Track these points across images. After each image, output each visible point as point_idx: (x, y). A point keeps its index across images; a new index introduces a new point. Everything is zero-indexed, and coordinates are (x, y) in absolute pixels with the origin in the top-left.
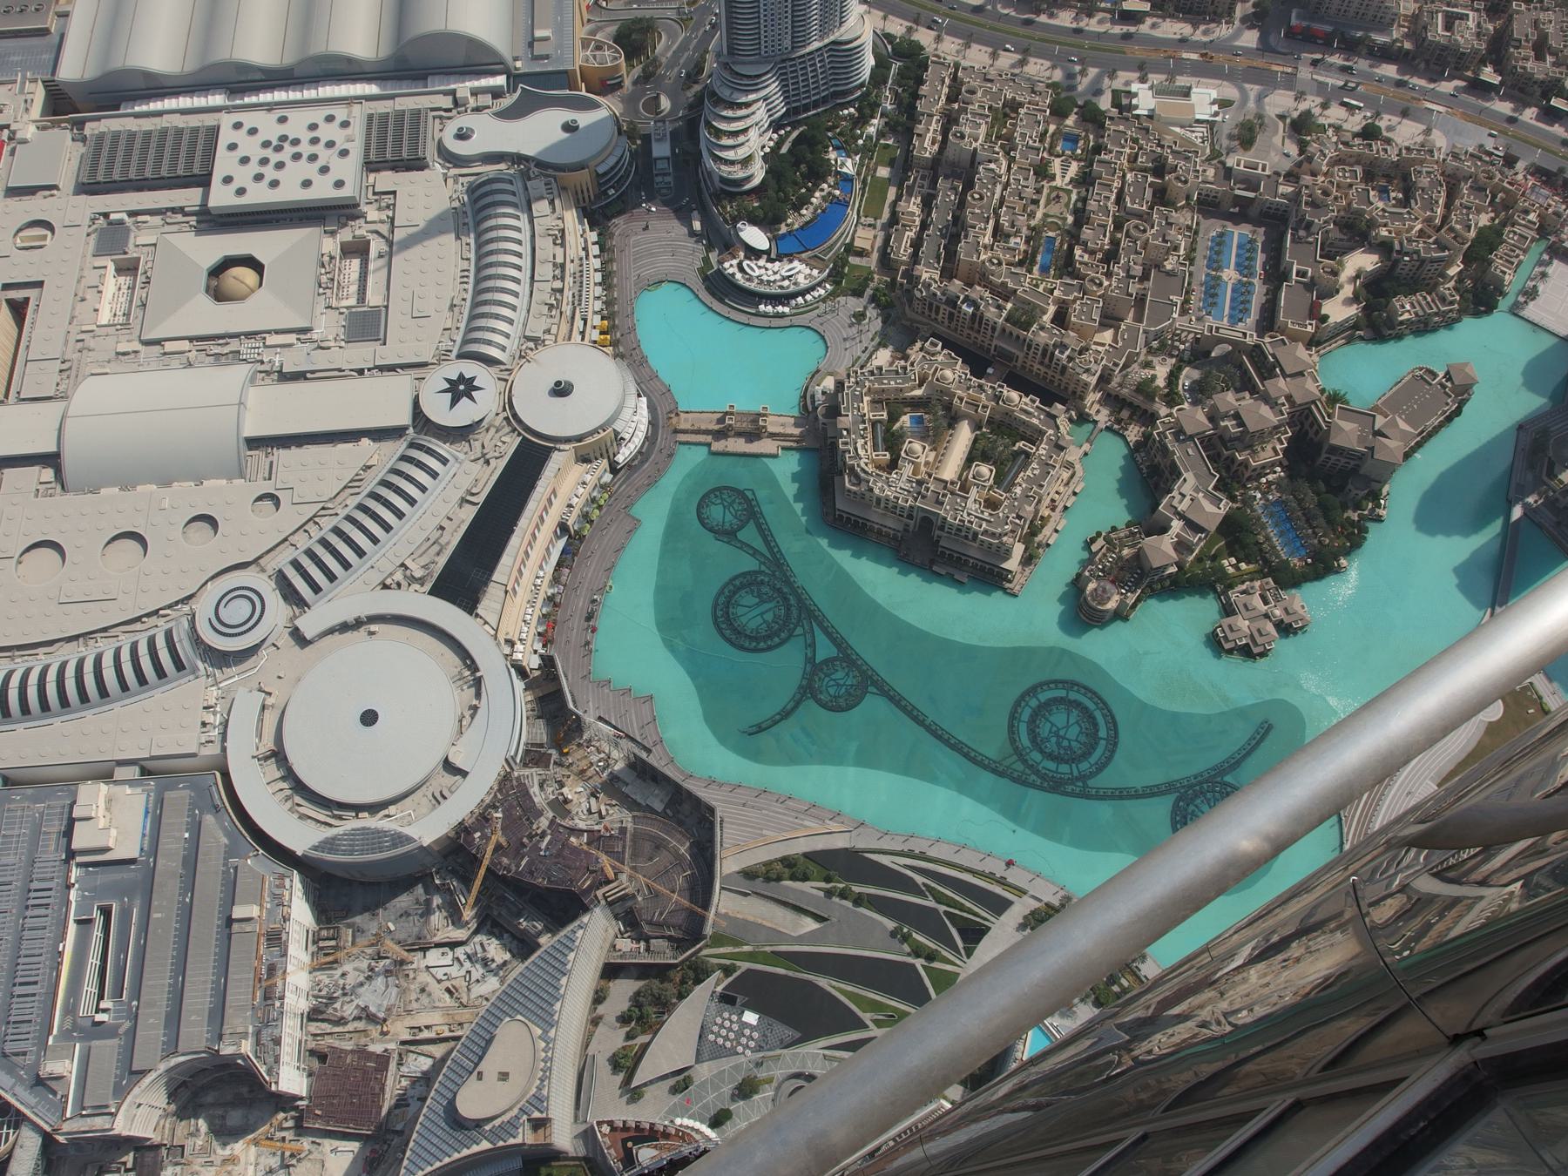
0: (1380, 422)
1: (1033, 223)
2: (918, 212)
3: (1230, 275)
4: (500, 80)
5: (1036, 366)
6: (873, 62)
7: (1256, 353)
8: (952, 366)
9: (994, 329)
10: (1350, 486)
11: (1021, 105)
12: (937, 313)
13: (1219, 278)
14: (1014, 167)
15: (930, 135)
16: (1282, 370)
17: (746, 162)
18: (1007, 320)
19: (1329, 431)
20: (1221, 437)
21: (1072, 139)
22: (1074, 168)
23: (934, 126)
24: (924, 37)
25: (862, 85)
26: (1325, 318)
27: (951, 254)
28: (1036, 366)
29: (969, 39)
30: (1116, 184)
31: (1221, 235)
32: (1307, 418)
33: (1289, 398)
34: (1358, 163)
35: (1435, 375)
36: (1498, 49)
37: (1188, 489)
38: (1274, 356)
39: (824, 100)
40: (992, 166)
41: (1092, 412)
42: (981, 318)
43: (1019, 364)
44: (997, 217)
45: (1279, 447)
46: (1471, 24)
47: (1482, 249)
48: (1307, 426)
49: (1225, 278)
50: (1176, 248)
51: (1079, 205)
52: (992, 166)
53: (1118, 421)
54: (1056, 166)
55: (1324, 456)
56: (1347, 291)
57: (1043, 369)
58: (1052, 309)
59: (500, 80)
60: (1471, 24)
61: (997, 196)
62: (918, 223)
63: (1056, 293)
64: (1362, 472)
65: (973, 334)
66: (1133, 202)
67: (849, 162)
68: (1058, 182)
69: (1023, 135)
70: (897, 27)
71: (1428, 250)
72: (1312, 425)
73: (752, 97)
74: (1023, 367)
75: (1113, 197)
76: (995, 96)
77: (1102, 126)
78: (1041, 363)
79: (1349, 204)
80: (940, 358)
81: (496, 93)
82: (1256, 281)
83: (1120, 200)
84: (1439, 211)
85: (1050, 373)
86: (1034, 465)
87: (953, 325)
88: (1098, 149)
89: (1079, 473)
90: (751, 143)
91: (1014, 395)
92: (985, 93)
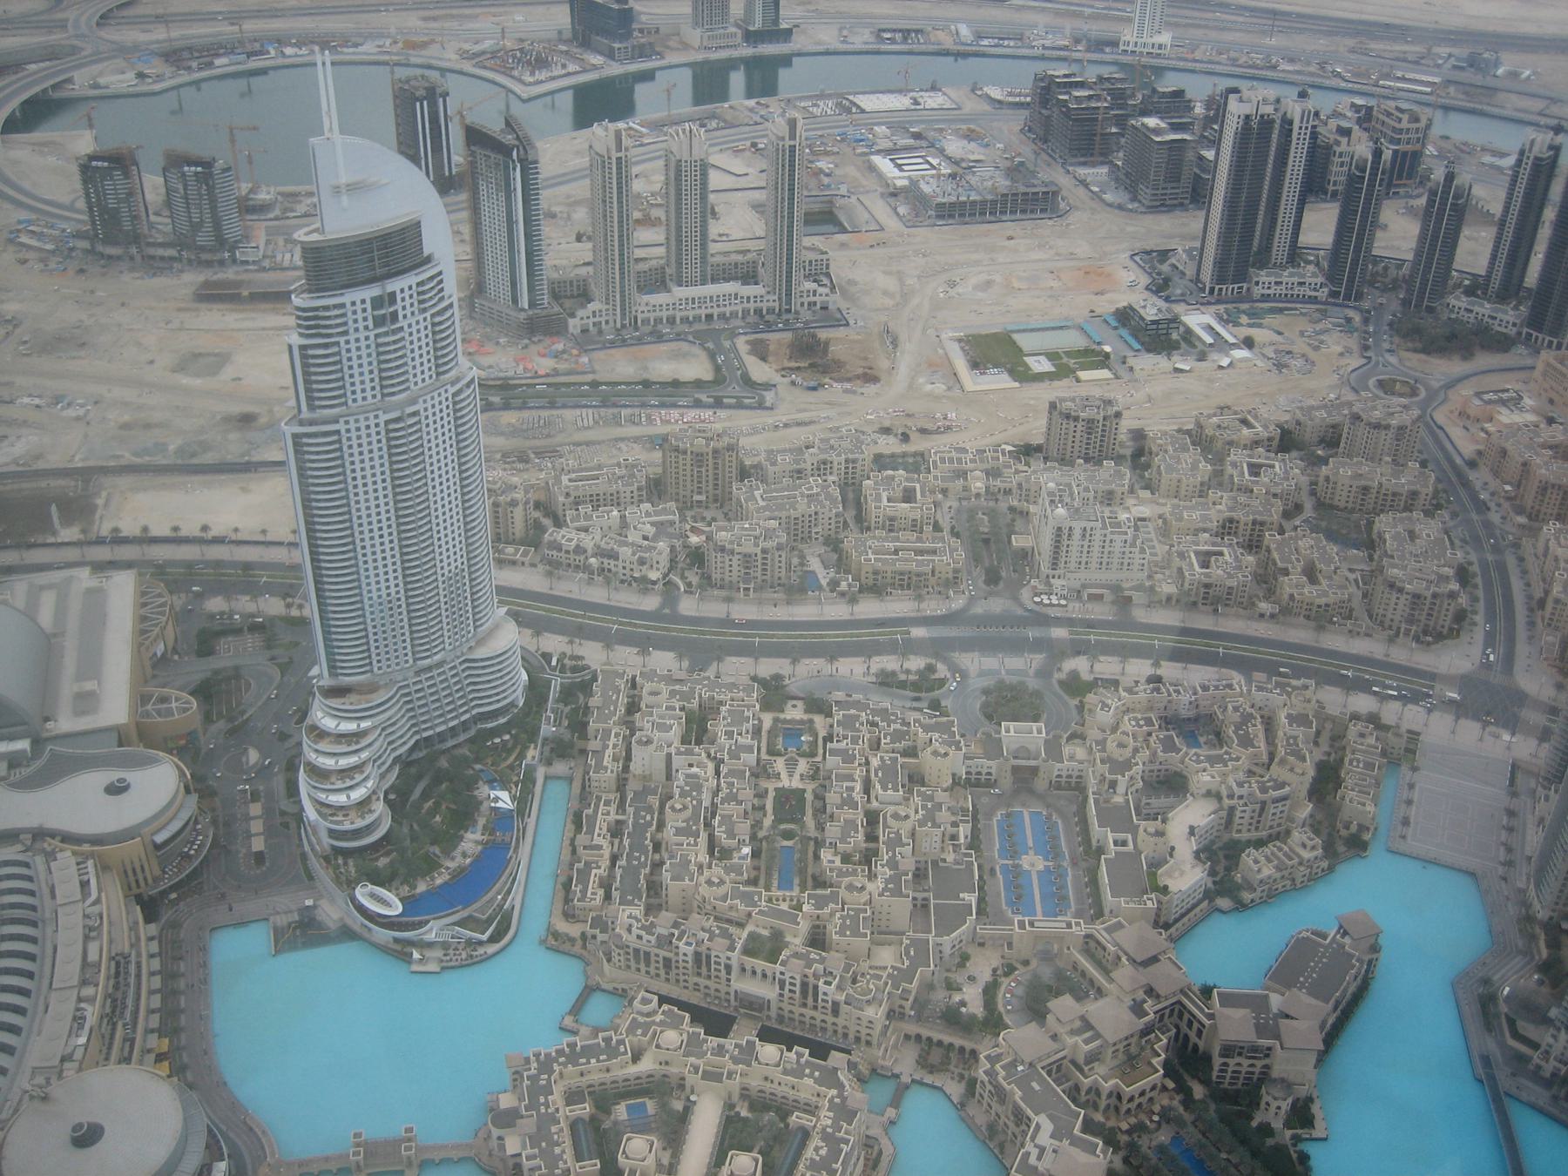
0: (1276, 1001)
1: (761, 834)
2: (605, 844)
3: (1033, 863)
4: (23, 745)
5: (798, 1010)
6: (525, 677)
7: (1091, 946)
8: (676, 1025)
9: (728, 968)
10: (1266, 1098)
11: (721, 703)
12: (648, 965)
13: (1017, 866)
14: (724, 770)
15: (609, 752)
16: (1130, 959)
17: (363, 805)
18: (747, 951)
19: (1214, 1027)
20: (1073, 1062)
21: (792, 731)
22: (803, 766)
23: (613, 740)
24: (593, 654)
25: (513, 704)
26: (1165, 890)
27: (654, 888)
28: (798, 1010)
29: (644, 644)
30: (859, 773)
31: (1008, 815)
32: (1181, 1016)
33: (1150, 991)
34: (1151, 709)
35: (1324, 937)
36: (1267, 578)
37: (1044, 1138)
38: (1117, 945)
39: (465, 726)
40: (695, 770)
41: (888, 1063)
42: (708, 957)
43: (773, 1013)
44: (708, 825)
45: (1155, 1061)
46: (1227, 557)
47: (1327, 780)
48: (1184, 1029)
49: (1026, 867)
50: (954, 837)
51: (819, 804)
52: (695, 770)
53: (932, 1069)
54: (780, 765)
55: (1217, 1061)
56: (1186, 849)
57: (809, 1012)
58: (804, 926)
59: (23, 745)
60: (1227, 557)
61: (706, 803)
62: (606, 853)
63: (805, 908)
64: (1275, 1074)
65: (702, 981)
66: (885, 789)
67: (504, 795)
68: (785, 782)
69: (729, 734)
70: (554, 644)
71: (1264, 790)
72: (1190, 1024)
73: (365, 724)
74: (781, 1019)
75: (858, 786)
76: (686, 697)
77: (829, 715)
78: (805, 1005)
79: (1154, 754)
80: (659, 1018)
81: (14, 761)
82: (1065, 864)
83: (867, 790)
84: (1263, 745)
85: (818, 1015)
86: (815, 1141)
87: (672, 976)
88: (829, 738)
89: (888, 1151)
90: (370, 784)
91: (769, 1051)
92: (673, 694)
